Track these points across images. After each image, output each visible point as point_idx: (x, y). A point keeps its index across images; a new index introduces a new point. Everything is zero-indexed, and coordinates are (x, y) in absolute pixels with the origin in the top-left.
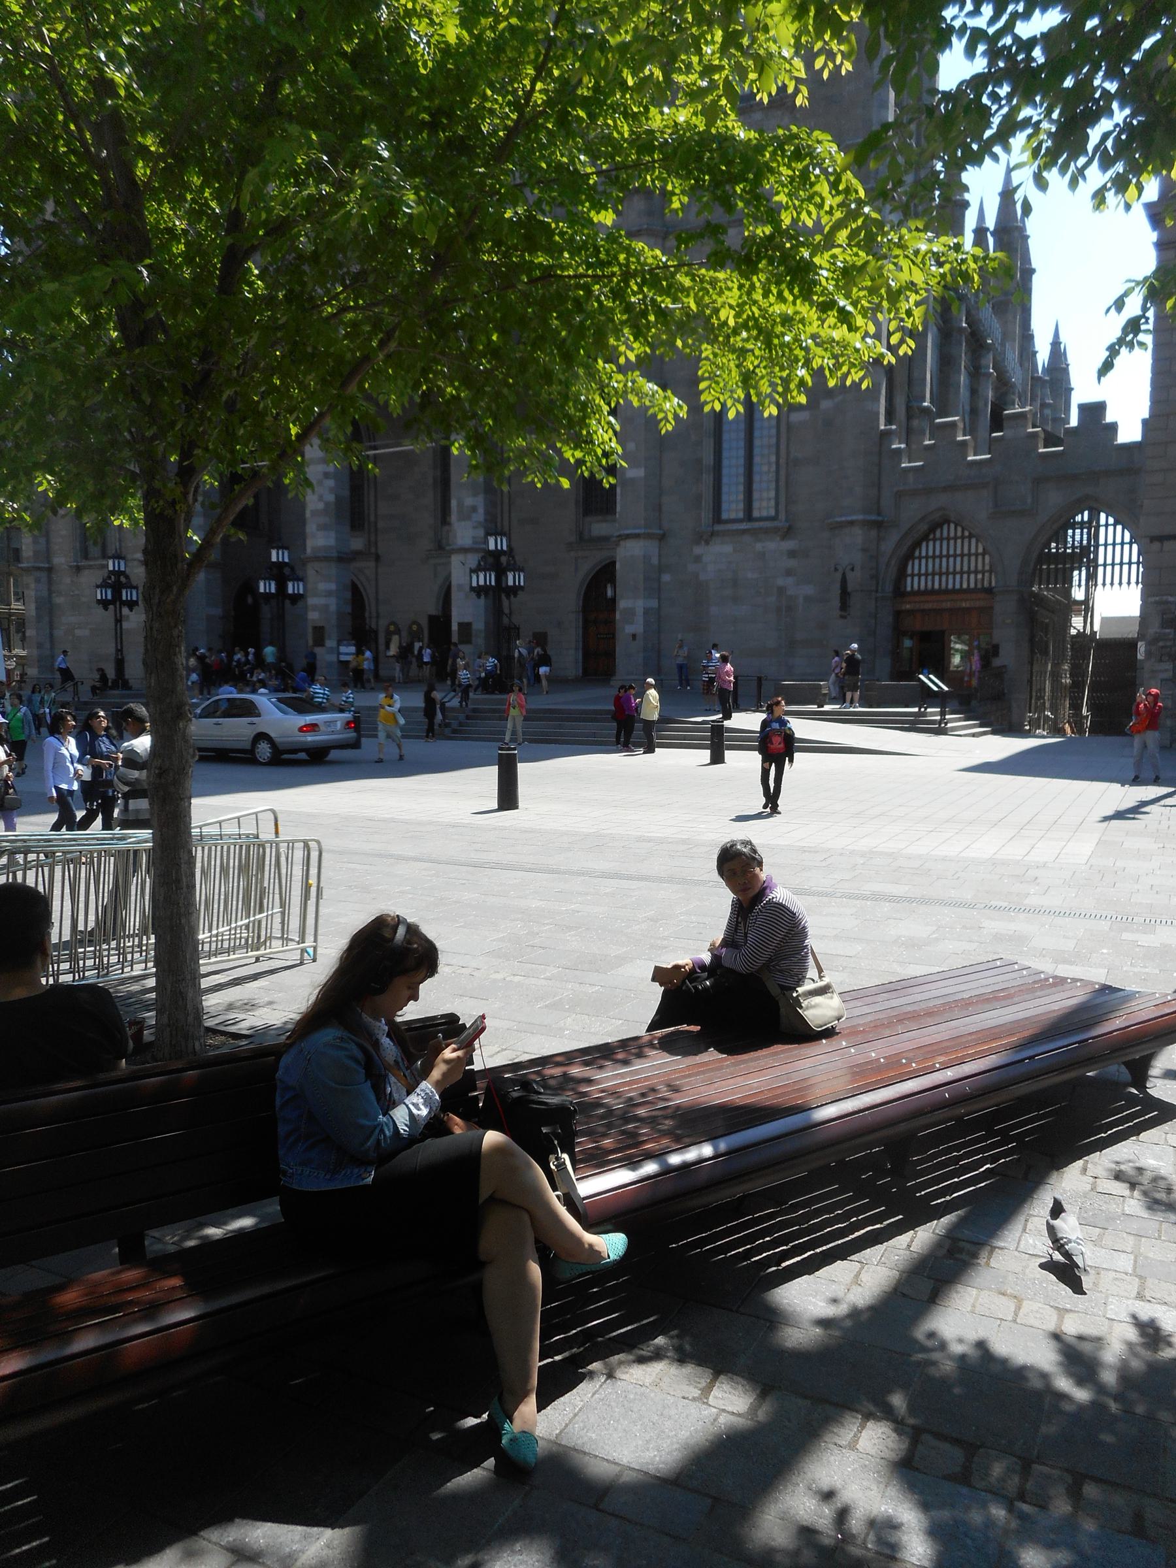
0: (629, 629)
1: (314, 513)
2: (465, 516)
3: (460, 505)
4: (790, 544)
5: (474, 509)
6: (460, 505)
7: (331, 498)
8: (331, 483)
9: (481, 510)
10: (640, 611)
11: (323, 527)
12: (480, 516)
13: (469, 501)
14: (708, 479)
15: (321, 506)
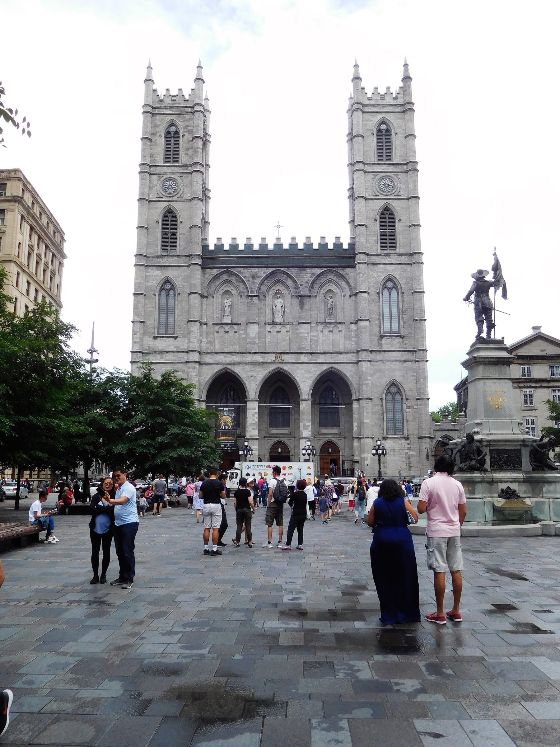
0: (366, 463)
1: (251, 424)
2: (306, 428)
3: (304, 425)
4: (408, 442)
5: (309, 426)
6: (304, 425)
7: (257, 420)
8: (257, 415)
9: (311, 427)
10: (369, 458)
11: (253, 429)
12: (310, 428)
13: (307, 424)
14: (385, 423)
15: (254, 422)
